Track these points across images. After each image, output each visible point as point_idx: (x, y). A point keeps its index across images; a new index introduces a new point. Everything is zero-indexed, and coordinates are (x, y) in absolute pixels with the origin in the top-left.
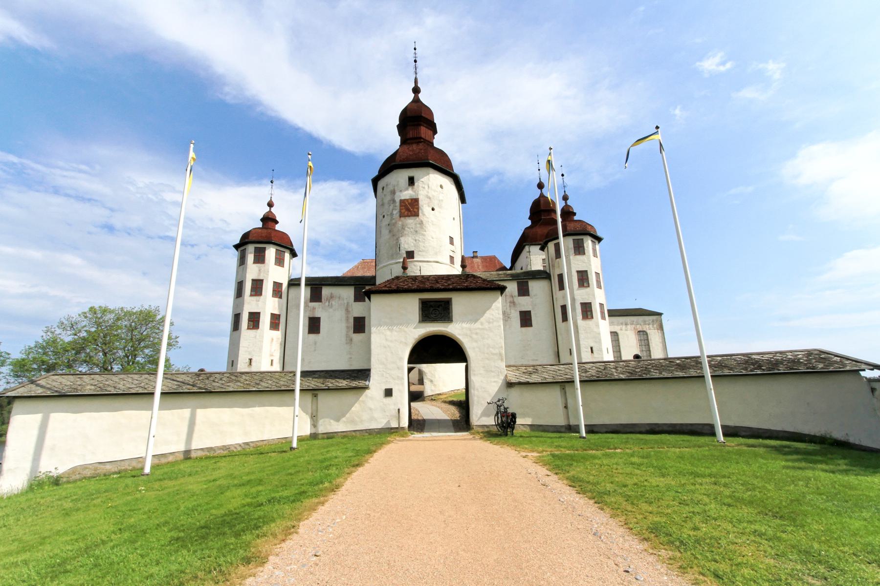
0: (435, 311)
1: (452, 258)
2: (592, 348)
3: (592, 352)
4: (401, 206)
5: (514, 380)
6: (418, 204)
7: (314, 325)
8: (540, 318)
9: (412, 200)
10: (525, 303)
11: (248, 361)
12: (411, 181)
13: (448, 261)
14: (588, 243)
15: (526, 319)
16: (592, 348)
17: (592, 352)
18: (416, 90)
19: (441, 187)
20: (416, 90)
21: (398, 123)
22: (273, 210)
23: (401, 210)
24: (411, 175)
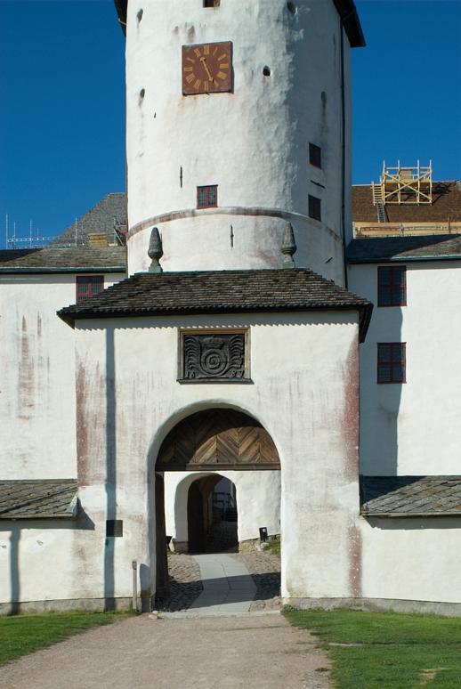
4: (185, 64)
23: (185, 74)
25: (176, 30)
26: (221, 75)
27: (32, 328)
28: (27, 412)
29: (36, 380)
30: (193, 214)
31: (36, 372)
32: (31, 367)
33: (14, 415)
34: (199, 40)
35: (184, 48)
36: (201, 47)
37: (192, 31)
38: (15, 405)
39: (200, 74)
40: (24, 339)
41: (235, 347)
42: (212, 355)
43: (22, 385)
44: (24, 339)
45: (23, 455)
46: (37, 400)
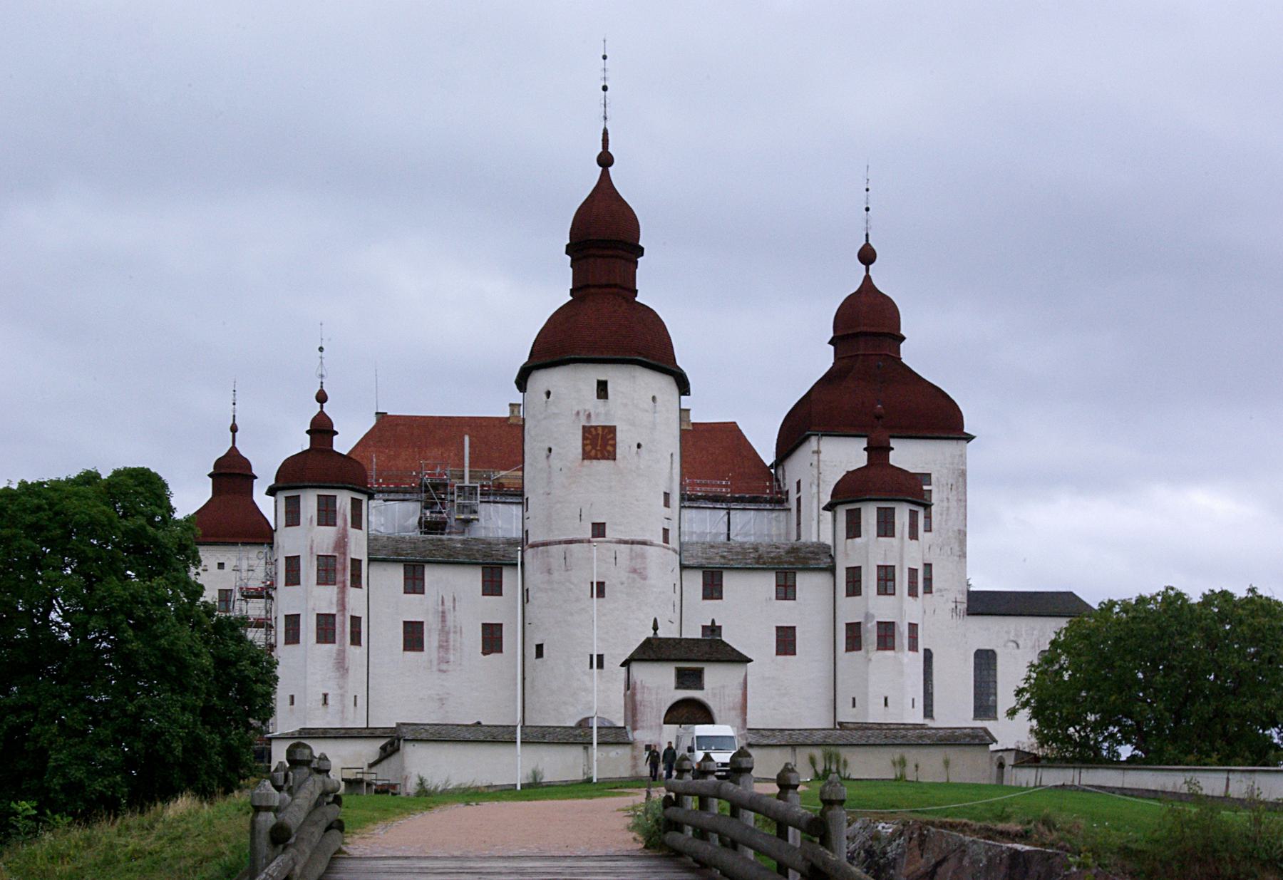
0: (689, 678)
1: (666, 531)
2: (886, 699)
3: (886, 704)
4: (584, 438)
5: (753, 741)
6: (614, 438)
7: (413, 636)
8: (811, 639)
9: (604, 427)
10: (786, 613)
11: (321, 697)
12: (602, 388)
13: (659, 539)
14: (902, 514)
15: (786, 641)
16: (886, 699)
17: (886, 704)
18: (605, 160)
19: (654, 398)
20: (605, 160)
21: (568, 242)
22: (327, 408)
23: (584, 445)
24: (603, 378)
25: (578, 413)
26: (609, 448)
27: (449, 604)
28: (444, 667)
29: (452, 643)
30: (589, 542)
31: (452, 635)
32: (448, 633)
33: (435, 668)
34: (594, 422)
35: (584, 427)
36: (596, 427)
37: (589, 416)
38: (435, 663)
39: (594, 446)
40: (443, 612)
41: (699, 674)
42: (689, 678)
43: (441, 647)
44: (443, 612)
45: (441, 699)
46: (452, 658)
